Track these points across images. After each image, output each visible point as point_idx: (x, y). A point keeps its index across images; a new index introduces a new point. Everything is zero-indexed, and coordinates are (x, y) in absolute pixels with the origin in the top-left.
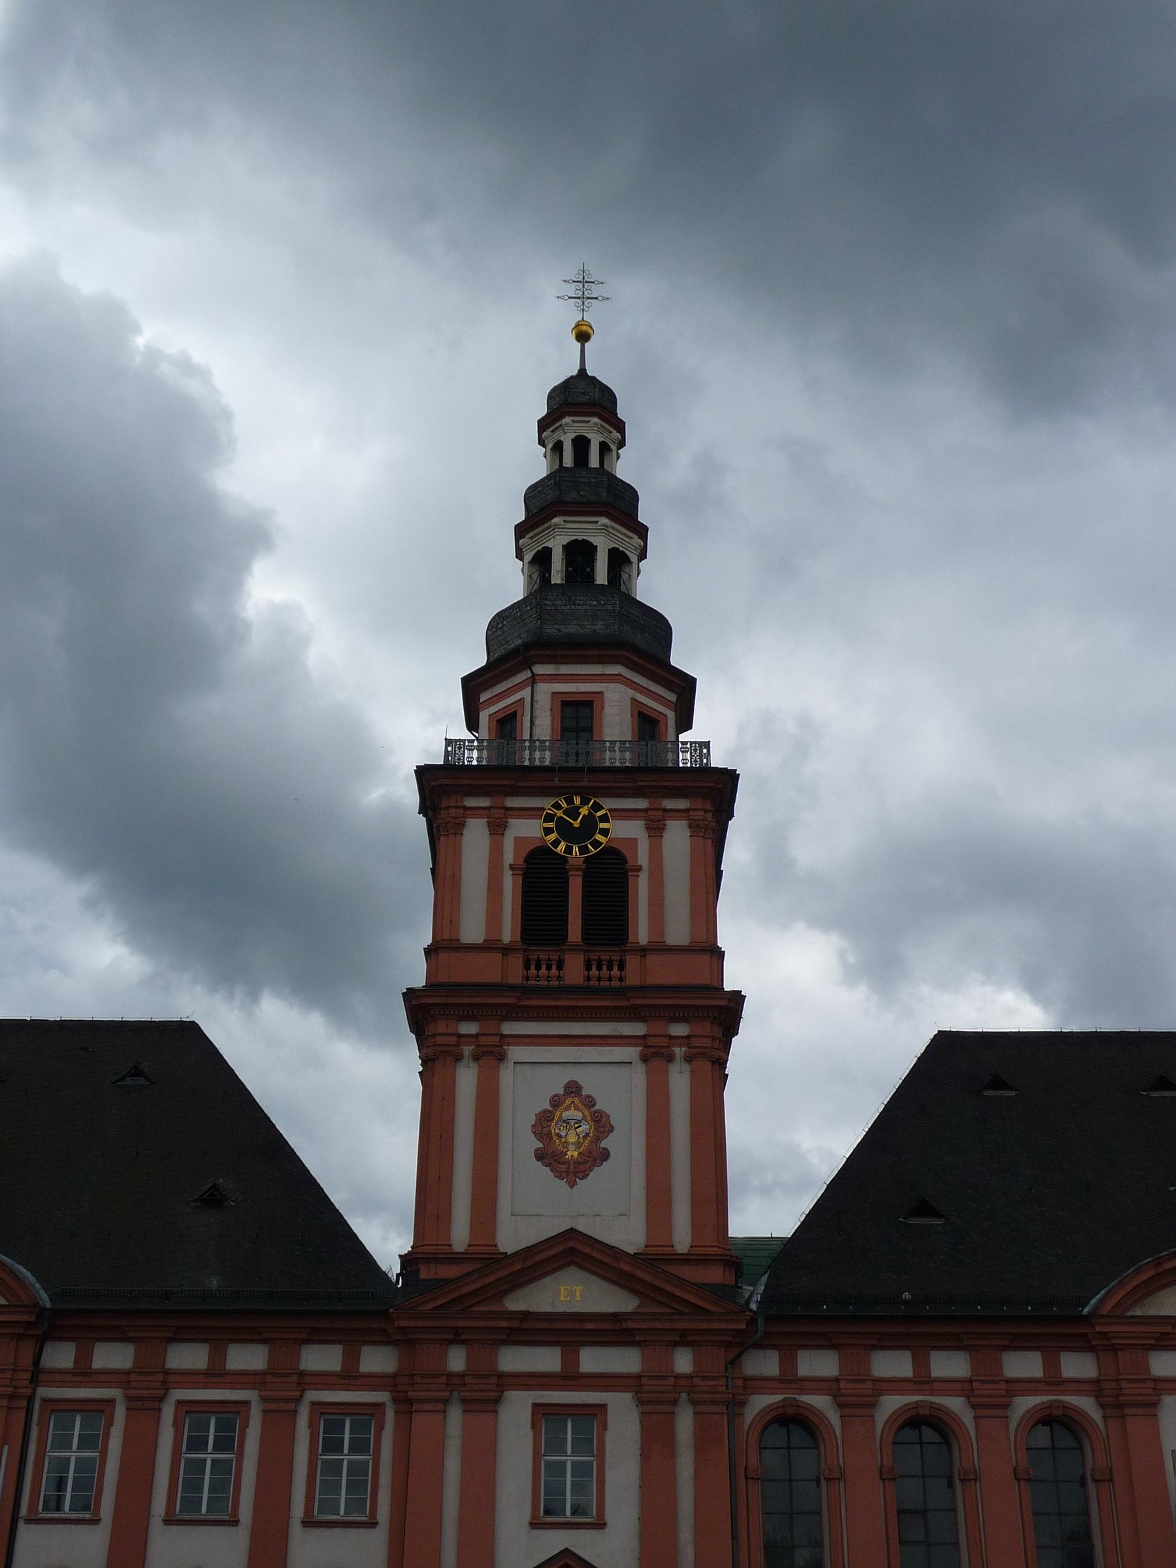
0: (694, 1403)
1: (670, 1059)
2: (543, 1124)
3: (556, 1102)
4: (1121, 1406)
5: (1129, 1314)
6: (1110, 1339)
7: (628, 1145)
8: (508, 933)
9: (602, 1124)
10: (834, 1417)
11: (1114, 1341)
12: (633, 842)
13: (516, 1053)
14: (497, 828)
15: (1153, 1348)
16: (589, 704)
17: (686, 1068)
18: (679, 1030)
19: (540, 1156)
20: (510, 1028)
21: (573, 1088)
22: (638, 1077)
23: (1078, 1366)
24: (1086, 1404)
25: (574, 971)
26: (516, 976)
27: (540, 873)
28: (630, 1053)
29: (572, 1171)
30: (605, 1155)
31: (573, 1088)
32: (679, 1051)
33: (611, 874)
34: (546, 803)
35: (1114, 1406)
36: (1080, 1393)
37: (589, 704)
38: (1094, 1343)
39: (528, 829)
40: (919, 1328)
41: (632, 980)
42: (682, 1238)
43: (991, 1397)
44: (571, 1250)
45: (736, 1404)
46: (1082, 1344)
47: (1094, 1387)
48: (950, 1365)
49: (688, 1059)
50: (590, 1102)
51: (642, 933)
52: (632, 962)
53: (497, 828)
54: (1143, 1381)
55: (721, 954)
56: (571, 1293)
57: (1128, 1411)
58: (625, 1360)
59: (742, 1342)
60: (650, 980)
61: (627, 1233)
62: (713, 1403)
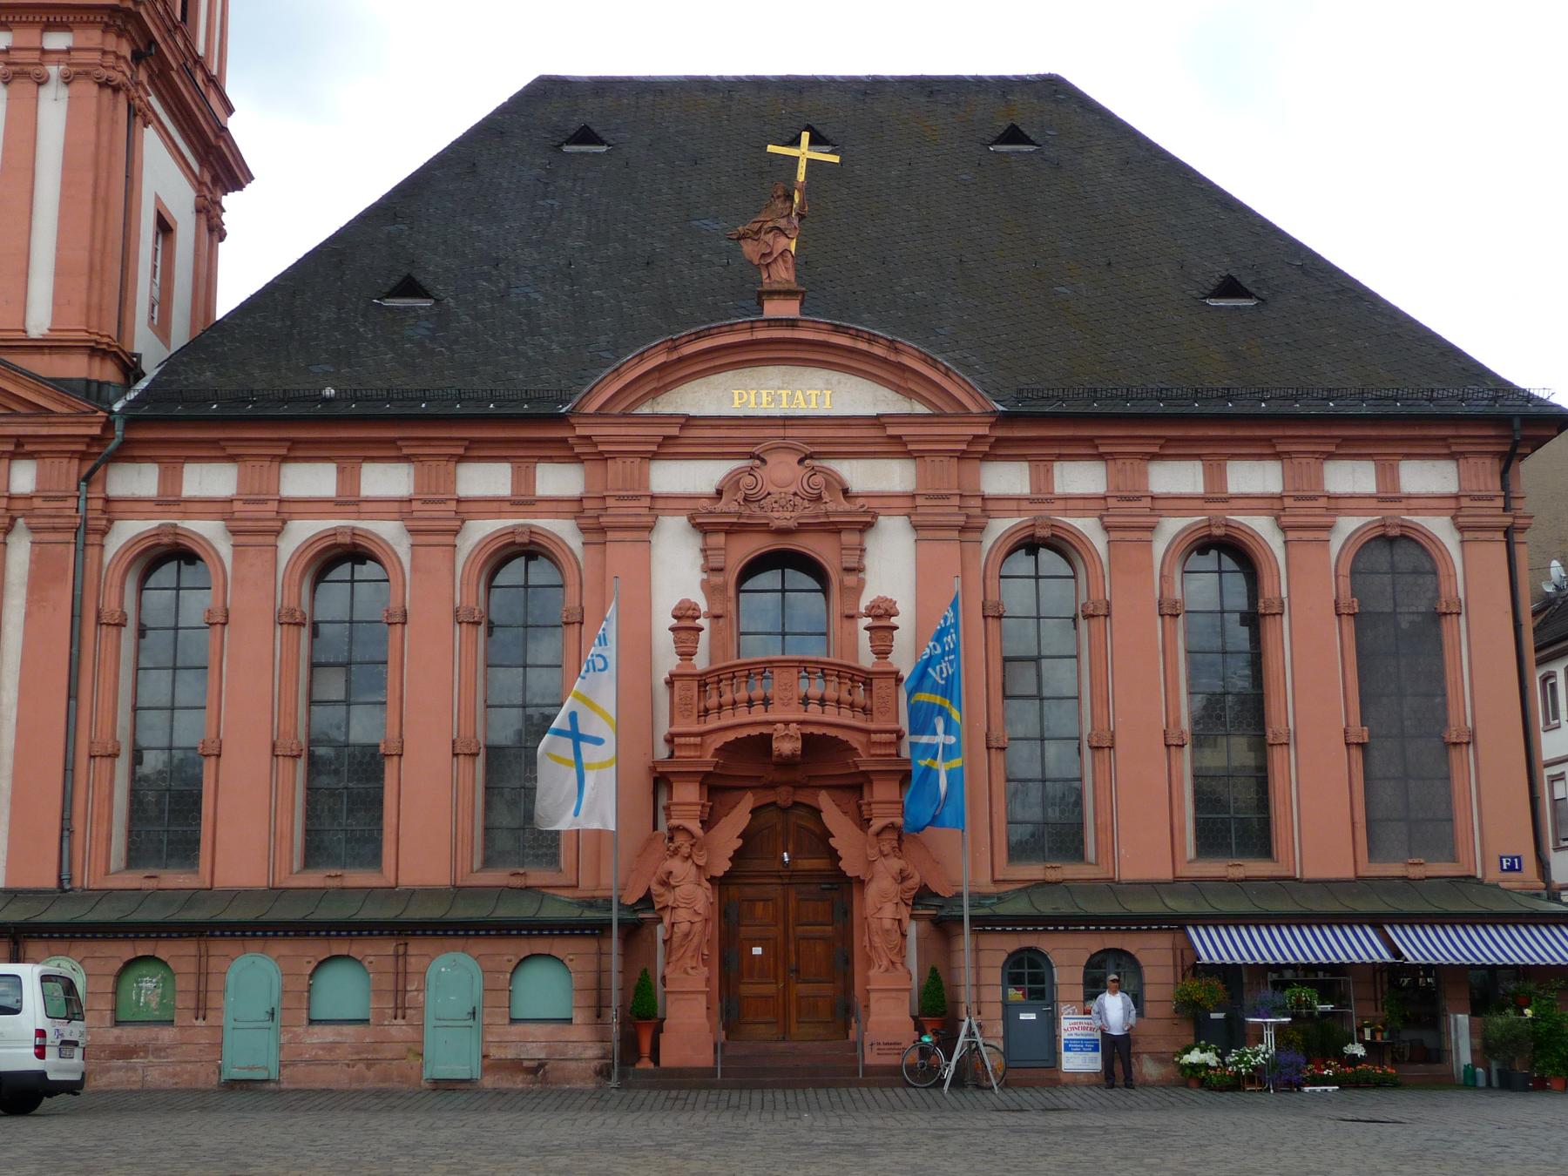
0: (33, 530)
1: (41, 81)
4: (603, 530)
5: (645, 409)
6: (596, 445)
11: (601, 448)
15: (655, 456)
17: (64, 92)
18: (57, 41)
23: (558, 480)
32: (54, 71)
35: (596, 531)
36: (556, 514)
38: (577, 450)
45: (89, 532)
46: (564, 452)
47: (575, 507)
49: (67, 80)
54: (636, 498)
57: (610, 535)
59: (99, 455)
62: (55, 529)
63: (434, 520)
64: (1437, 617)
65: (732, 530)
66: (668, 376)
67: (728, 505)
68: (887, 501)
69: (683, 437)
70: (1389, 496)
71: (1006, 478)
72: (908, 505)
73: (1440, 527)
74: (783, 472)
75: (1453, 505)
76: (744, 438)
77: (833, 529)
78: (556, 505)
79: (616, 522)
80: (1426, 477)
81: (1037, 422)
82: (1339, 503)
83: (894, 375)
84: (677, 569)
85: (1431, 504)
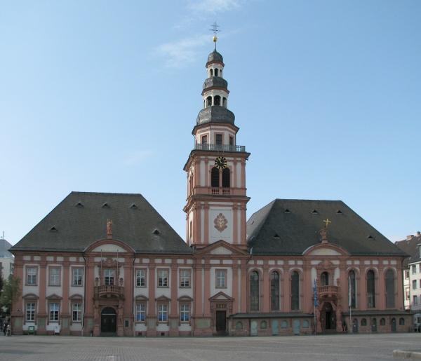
1: (237, 209)
2: (216, 221)
3: (218, 217)
7: (230, 225)
8: (209, 184)
9: (226, 221)
10: (262, 271)
12: (231, 167)
13: (211, 208)
14: (206, 163)
16: (221, 135)
18: (239, 204)
19: (215, 227)
20: (210, 203)
21: (221, 214)
22: (232, 212)
23: (300, 263)
24: (301, 269)
25: (221, 193)
26: (211, 193)
27: (214, 172)
28: (231, 208)
29: (221, 229)
30: (226, 227)
31: (221, 214)
33: (227, 173)
34: (215, 158)
37: (221, 135)
39: (212, 163)
40: (275, 255)
41: (231, 194)
42: (239, 242)
43: (265, 267)
44: (221, 243)
45: (247, 270)
46: (301, 259)
47: (302, 266)
48: (280, 262)
50: (224, 217)
51: (232, 185)
52: (231, 191)
53: (206, 163)
55: (246, 189)
56: (221, 251)
58: (230, 262)
59: (249, 259)
60: (235, 194)
61: (230, 241)
63: (286, 267)
64: (394, 279)
65: (321, 269)
66: (315, 249)
67: (320, 267)
68: (336, 266)
69: (316, 258)
70: (389, 264)
71: (349, 263)
72: (339, 266)
73: (395, 269)
74: (326, 262)
75: (396, 266)
76: (322, 258)
77: (332, 269)
78: (300, 266)
79: (307, 268)
80: (394, 262)
81: (354, 255)
82: (385, 266)
83: (338, 250)
84: (314, 275)
85: (394, 266)
